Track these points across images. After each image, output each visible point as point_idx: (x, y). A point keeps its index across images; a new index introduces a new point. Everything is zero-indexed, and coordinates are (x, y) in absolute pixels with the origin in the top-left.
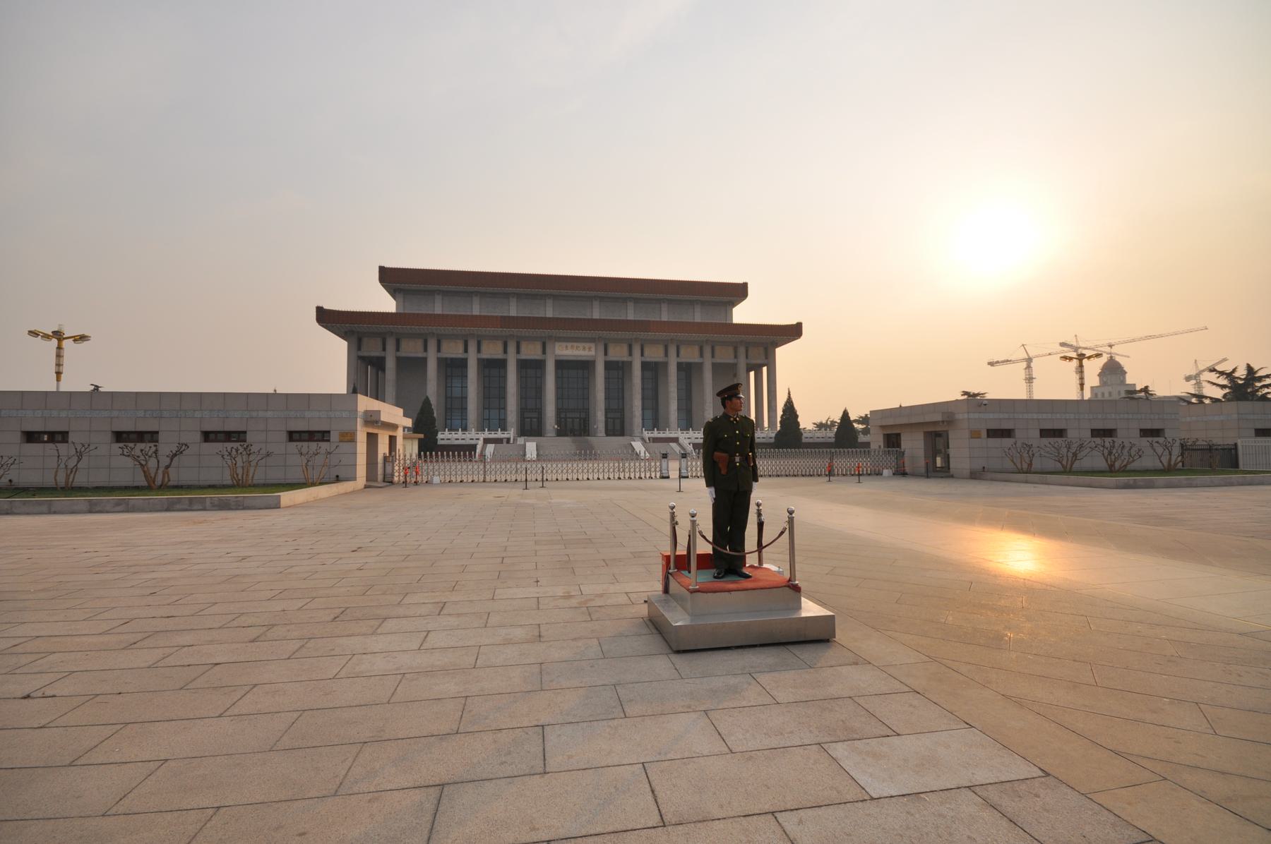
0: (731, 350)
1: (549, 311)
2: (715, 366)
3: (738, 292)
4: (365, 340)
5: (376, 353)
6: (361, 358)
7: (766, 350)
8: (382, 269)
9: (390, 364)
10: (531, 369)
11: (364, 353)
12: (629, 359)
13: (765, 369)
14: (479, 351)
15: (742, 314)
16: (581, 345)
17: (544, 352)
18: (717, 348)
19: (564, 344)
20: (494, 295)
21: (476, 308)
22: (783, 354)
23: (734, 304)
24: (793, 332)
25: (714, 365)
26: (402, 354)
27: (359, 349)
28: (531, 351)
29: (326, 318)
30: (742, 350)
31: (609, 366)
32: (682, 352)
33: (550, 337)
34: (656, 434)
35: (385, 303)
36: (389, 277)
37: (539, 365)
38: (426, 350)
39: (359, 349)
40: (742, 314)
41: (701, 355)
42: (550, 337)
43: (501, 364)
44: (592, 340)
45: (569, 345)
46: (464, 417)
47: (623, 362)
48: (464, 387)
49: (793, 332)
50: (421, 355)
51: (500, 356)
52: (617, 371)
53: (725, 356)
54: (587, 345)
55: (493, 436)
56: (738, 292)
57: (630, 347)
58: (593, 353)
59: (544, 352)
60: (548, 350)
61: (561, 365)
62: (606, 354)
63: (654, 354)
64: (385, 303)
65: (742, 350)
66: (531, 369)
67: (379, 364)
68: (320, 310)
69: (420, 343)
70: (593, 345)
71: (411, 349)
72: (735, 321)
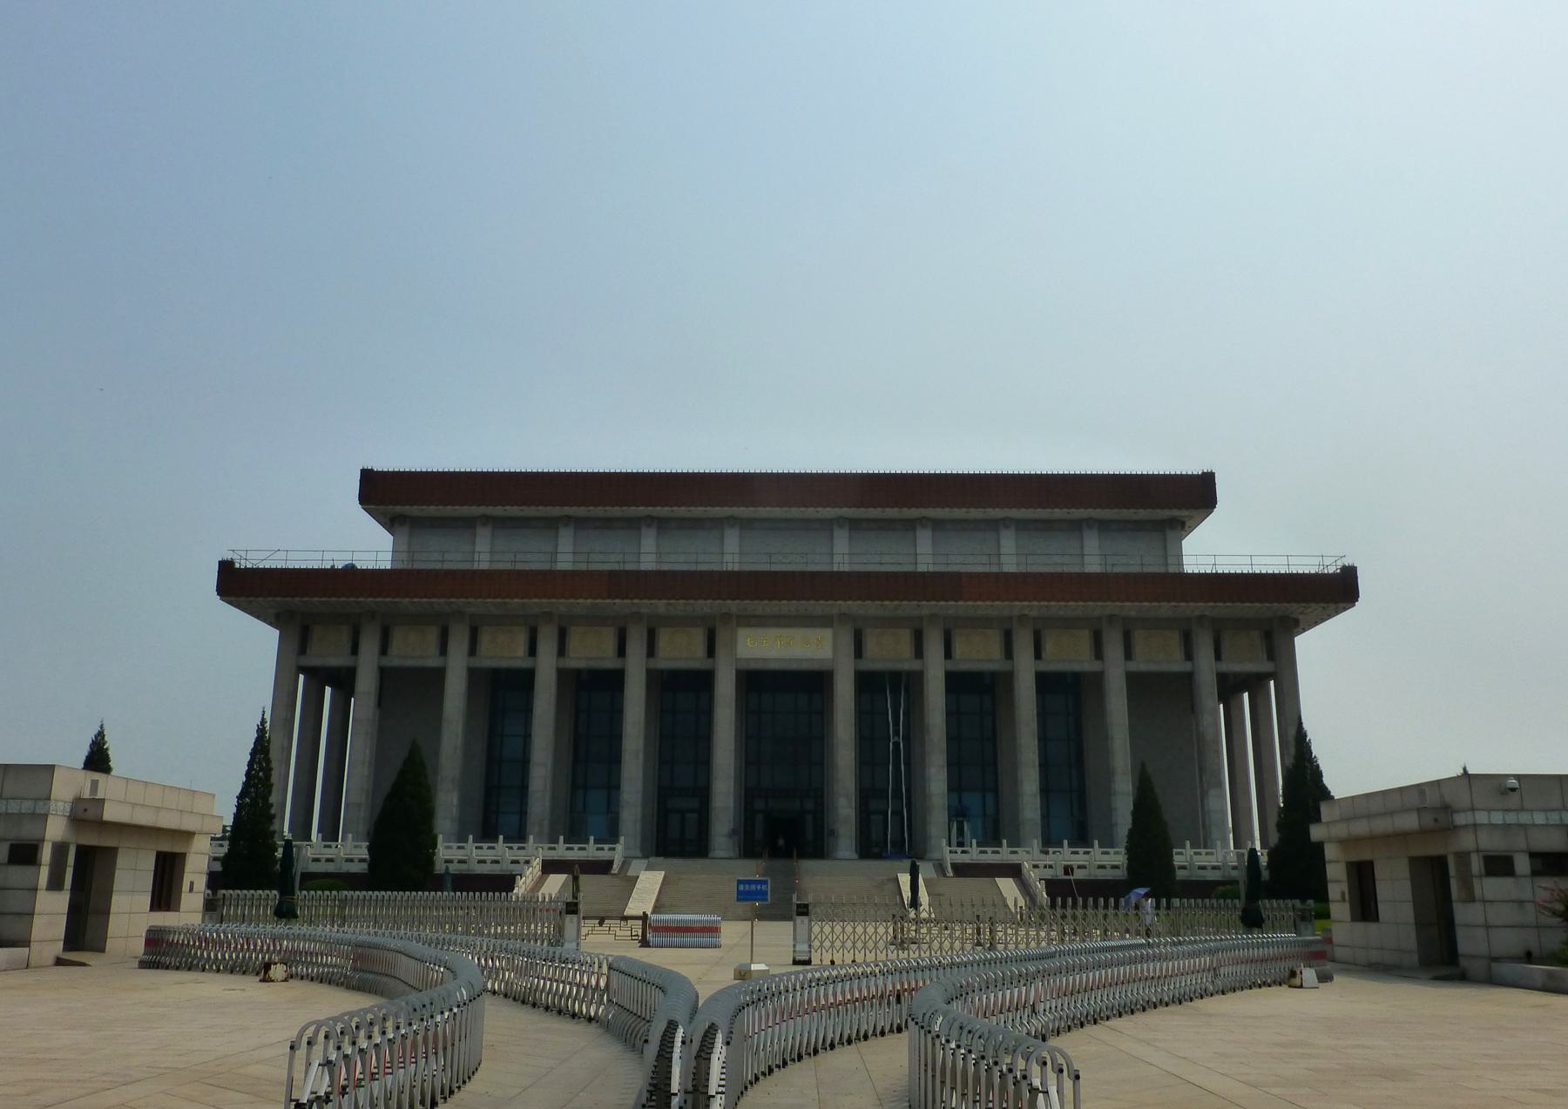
0: (1174, 639)
1: (731, 553)
2: (1136, 682)
3: (1193, 495)
5: (338, 660)
6: (309, 671)
7: (1268, 636)
9: (366, 682)
10: (682, 693)
12: (915, 665)
14: (562, 651)
15: (1207, 548)
16: (799, 633)
17: (711, 652)
18: (1139, 636)
20: (607, 523)
21: (566, 553)
22: (1318, 650)
24: (1336, 590)
26: (393, 660)
27: (303, 650)
28: (682, 650)
29: (238, 584)
31: (867, 683)
32: (1049, 647)
33: (726, 617)
34: (974, 854)
35: (370, 545)
36: (380, 491)
37: (703, 681)
38: (443, 651)
39: (303, 650)
40: (1207, 548)
41: (1099, 654)
42: (726, 617)
43: (613, 681)
44: (824, 621)
46: (523, 814)
47: (993, 674)
48: (527, 737)
49: (1336, 590)
50: (433, 662)
51: (610, 663)
53: (1159, 656)
55: (575, 854)
56: (1193, 495)
59: (711, 652)
61: (754, 681)
62: (859, 653)
63: (978, 653)
66: (682, 693)
67: (344, 681)
68: (226, 568)
70: (827, 633)
71: (414, 649)
72: (1188, 569)
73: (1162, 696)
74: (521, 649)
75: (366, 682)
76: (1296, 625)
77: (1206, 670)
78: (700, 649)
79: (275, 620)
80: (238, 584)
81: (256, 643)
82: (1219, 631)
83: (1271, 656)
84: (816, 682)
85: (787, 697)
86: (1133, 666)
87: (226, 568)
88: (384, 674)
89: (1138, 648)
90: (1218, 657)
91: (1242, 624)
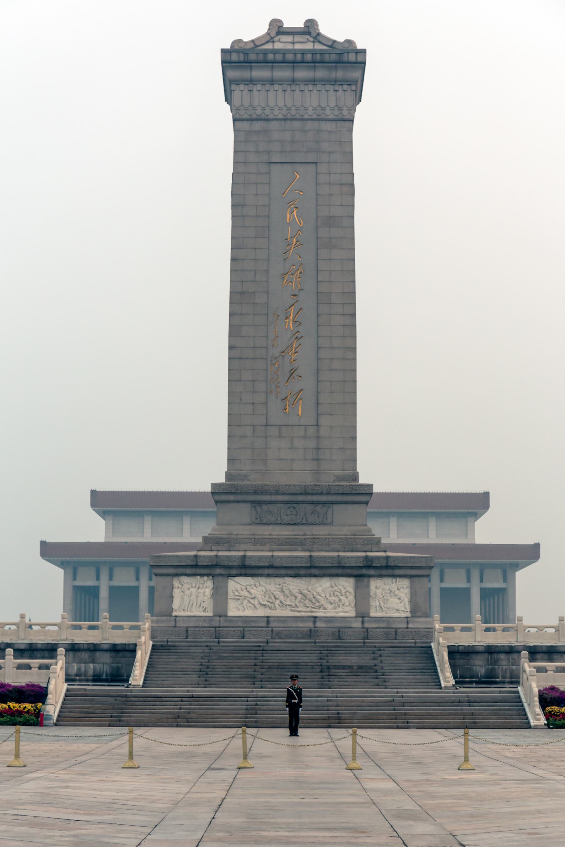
0: (462, 573)
4: (80, 570)
9: (104, 593)
11: (79, 583)
18: (447, 571)
23: (476, 516)
25: (442, 590)
26: (115, 583)
27: (75, 579)
29: (49, 551)
30: (475, 574)
39: (75, 579)
49: (531, 553)
50: (133, 583)
65: (475, 574)
67: (94, 592)
68: (43, 544)
69: (132, 571)
75: (104, 593)
76: (517, 567)
79: (62, 565)
80: (49, 551)
81: (55, 576)
82: (482, 569)
83: (505, 580)
86: (444, 585)
87: (43, 544)
88: (112, 589)
89: (446, 577)
90: (481, 581)
91: (494, 566)
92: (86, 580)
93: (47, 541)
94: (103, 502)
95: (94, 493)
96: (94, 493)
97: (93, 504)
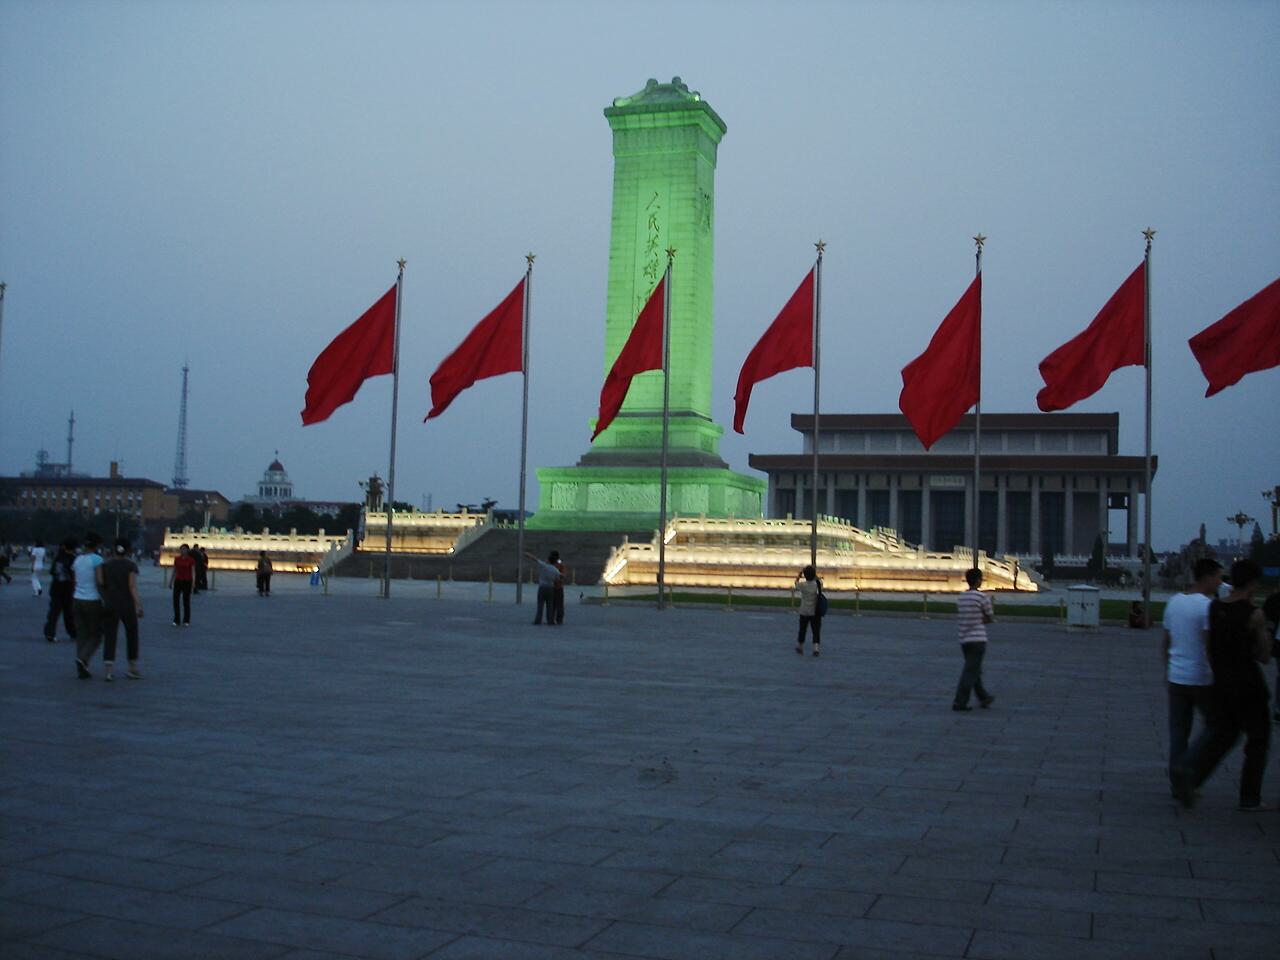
2: (1077, 496)
8: (793, 416)
11: (780, 487)
13: (1126, 499)
17: (921, 484)
19: (938, 477)
28: (910, 483)
32: (1045, 482)
37: (919, 493)
39: (777, 482)
45: (942, 478)
52: (988, 499)
53: (1086, 486)
54: (958, 478)
57: (997, 479)
58: (963, 484)
59: (921, 484)
60: (925, 484)
61: (937, 495)
64: (795, 444)
70: (963, 479)
73: (1088, 504)
74: (853, 484)
77: (1103, 491)
78: (917, 483)
84: (960, 495)
85: (947, 501)
92: (786, 484)
93: (755, 454)
94: (799, 422)
95: (794, 416)
96: (794, 416)
97: (794, 425)
